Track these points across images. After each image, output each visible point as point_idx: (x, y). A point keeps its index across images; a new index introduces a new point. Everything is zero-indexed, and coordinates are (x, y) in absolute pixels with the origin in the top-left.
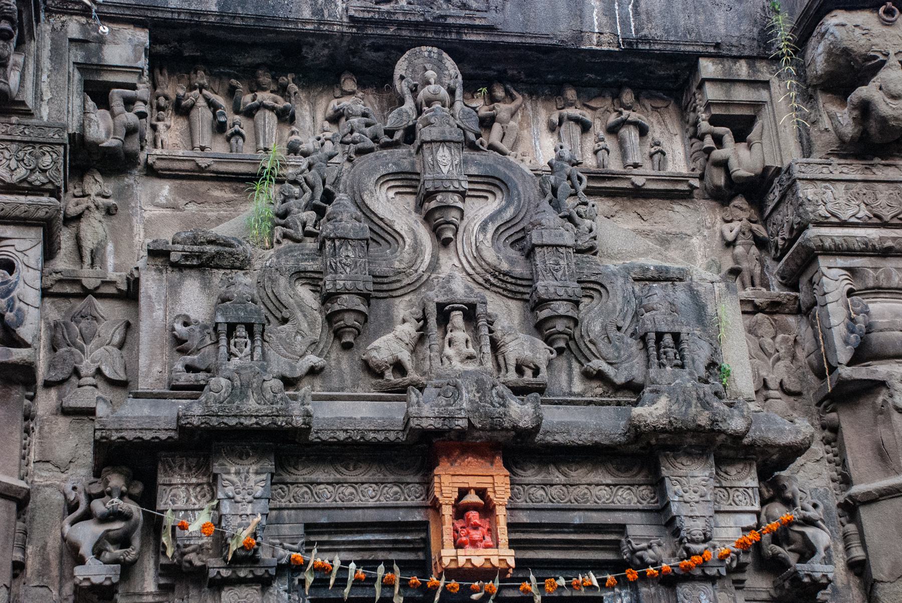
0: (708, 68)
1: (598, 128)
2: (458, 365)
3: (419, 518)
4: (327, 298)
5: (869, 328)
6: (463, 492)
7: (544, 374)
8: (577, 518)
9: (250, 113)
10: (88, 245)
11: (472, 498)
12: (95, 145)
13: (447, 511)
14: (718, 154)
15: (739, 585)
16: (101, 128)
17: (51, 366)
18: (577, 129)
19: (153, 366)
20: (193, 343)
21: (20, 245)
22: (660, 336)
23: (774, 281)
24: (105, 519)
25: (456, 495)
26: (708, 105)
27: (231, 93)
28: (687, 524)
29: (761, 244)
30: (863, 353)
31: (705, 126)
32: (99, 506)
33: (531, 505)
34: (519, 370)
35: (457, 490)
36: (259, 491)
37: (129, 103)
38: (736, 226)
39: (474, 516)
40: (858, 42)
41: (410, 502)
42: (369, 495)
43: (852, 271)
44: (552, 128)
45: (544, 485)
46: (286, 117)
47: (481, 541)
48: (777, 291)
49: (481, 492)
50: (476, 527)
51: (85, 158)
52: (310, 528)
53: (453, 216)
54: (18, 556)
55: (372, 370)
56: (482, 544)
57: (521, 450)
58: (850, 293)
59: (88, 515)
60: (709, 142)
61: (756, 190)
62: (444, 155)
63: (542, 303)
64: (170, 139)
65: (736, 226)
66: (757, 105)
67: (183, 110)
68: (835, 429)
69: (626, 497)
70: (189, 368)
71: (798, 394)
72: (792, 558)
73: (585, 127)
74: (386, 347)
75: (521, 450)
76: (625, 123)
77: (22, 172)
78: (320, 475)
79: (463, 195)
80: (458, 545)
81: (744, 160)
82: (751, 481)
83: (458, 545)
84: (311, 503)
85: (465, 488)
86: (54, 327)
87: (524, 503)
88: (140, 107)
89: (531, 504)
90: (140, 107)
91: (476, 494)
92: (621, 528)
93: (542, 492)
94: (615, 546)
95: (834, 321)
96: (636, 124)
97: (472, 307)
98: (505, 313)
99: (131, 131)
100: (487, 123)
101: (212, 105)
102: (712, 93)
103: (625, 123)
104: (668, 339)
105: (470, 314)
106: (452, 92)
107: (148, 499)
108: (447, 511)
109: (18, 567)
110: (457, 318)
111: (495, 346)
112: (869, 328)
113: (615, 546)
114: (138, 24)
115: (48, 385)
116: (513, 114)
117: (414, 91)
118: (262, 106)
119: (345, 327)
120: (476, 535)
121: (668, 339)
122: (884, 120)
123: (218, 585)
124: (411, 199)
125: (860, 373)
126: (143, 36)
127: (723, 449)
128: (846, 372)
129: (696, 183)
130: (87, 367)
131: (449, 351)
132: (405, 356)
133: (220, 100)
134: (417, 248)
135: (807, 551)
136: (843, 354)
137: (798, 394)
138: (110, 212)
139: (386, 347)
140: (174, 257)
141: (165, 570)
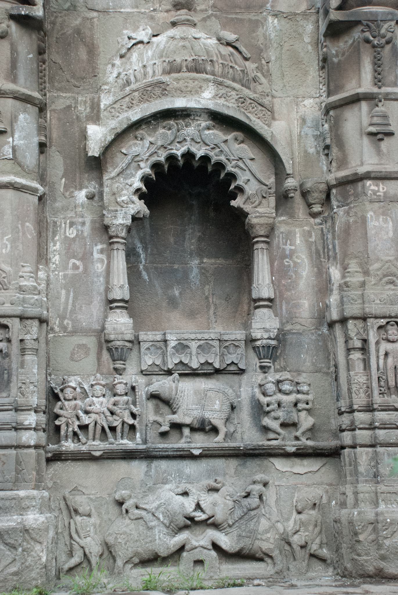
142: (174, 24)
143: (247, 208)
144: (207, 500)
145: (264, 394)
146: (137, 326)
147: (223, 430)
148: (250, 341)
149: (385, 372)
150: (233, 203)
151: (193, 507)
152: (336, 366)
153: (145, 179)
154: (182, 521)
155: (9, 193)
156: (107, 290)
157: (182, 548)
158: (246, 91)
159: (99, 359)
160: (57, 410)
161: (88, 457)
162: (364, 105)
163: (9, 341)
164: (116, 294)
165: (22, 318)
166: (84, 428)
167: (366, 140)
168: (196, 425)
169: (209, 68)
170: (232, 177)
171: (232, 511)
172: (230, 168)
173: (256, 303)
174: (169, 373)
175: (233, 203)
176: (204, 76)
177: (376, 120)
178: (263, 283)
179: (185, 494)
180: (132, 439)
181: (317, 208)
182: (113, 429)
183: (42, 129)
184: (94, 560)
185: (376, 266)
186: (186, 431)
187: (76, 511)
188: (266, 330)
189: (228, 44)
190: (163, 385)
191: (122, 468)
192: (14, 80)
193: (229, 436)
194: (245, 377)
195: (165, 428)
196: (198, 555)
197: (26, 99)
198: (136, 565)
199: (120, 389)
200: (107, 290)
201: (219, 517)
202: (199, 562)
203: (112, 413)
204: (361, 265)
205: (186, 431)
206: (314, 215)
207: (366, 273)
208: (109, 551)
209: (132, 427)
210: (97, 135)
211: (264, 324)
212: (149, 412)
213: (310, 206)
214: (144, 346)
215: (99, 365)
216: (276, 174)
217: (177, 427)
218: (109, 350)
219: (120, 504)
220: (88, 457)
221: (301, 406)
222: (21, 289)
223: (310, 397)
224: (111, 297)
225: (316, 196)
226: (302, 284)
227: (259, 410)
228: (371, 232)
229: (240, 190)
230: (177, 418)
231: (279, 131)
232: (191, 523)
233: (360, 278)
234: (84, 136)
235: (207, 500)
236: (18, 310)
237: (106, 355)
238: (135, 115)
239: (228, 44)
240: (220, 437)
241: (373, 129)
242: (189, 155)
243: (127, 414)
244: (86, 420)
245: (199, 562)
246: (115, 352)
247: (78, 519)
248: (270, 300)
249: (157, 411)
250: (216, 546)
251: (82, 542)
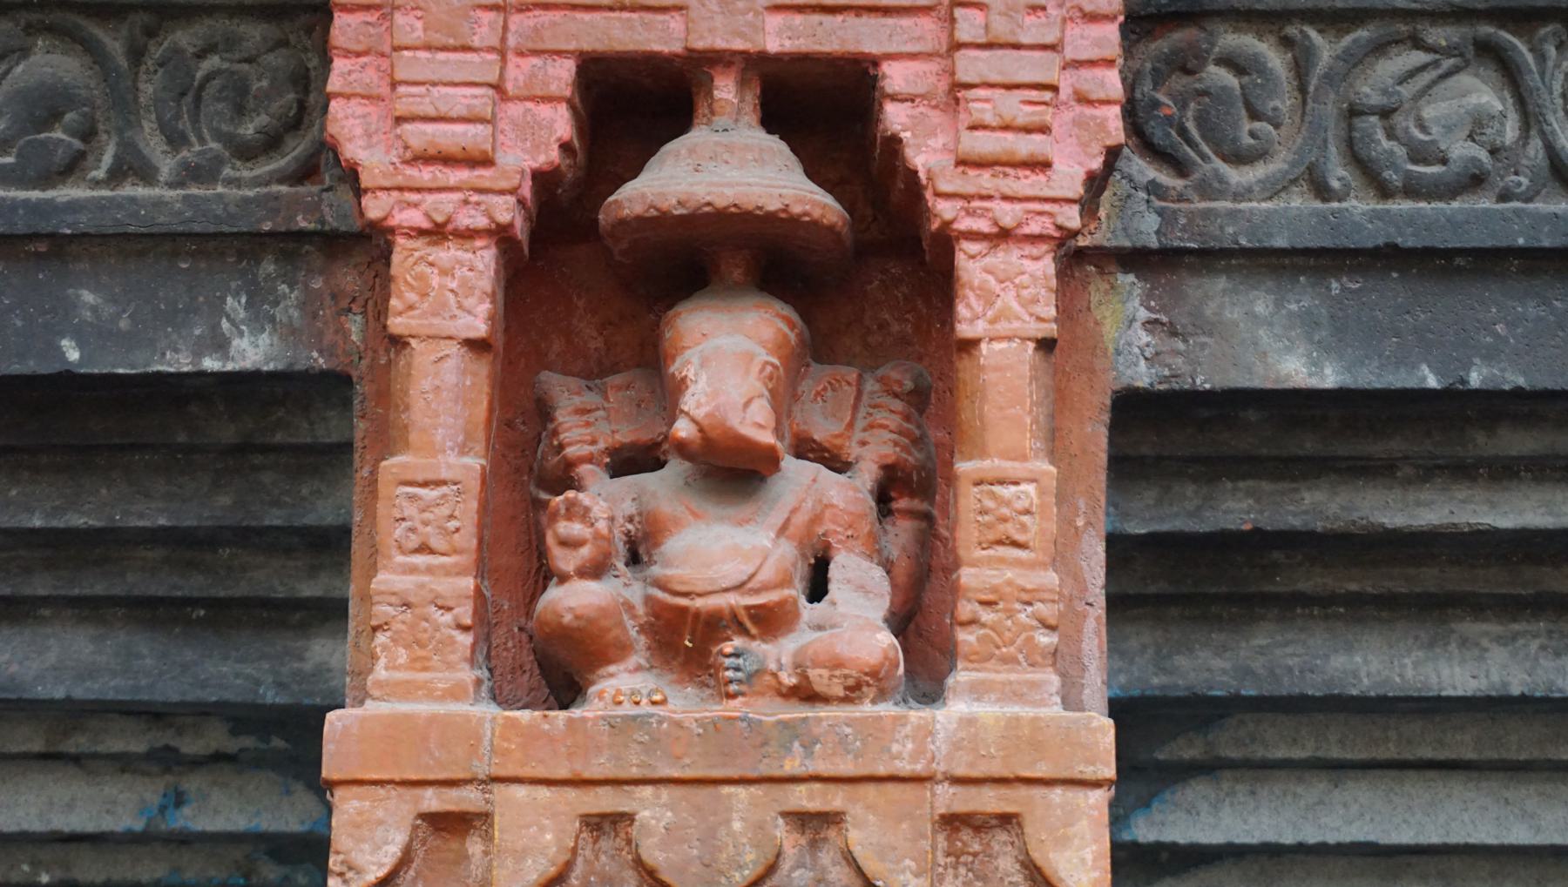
3: (252, 351)
6: (633, 104)
11: (731, 166)
25: (541, 134)
33: (1360, 210)
35: (562, 74)
39: (727, 359)
41: (160, 197)
47: (770, 621)
49: (823, 107)
50: (733, 471)
56: (778, 654)
85: (651, 63)
87: (1299, 202)
89: (1360, 205)
91: (771, 121)
93: (1480, 93)
108: (447, 297)
120: (721, 551)
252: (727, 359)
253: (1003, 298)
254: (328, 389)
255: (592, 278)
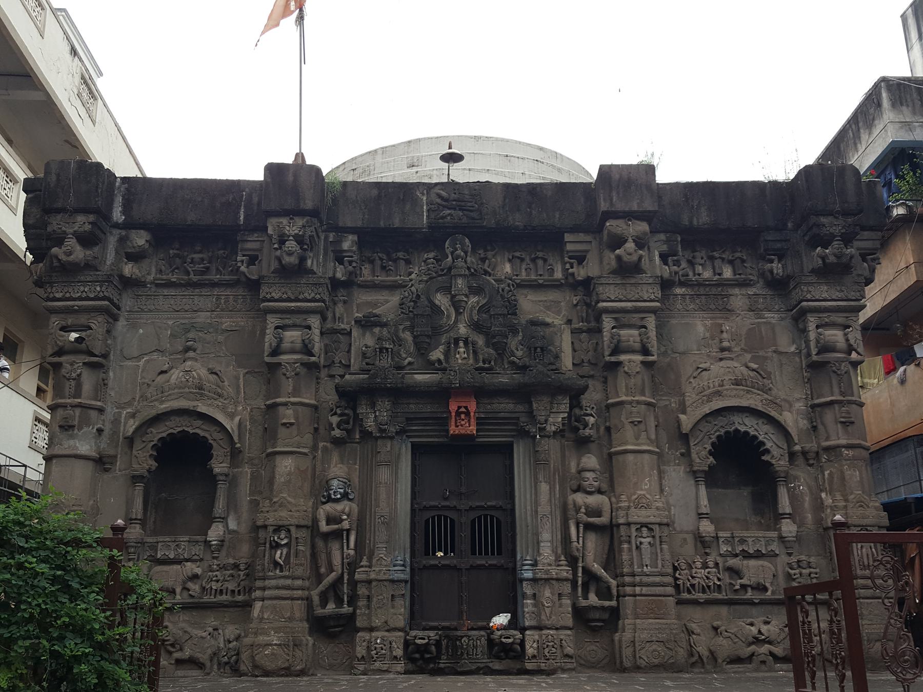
0: (568, 237)
1: (528, 260)
2: (460, 361)
4: (415, 337)
5: (619, 341)
6: (459, 407)
7: (493, 363)
8: (502, 415)
9: (395, 261)
10: (337, 315)
11: (463, 410)
12: (339, 280)
13: (453, 414)
14: (571, 270)
15: (563, 436)
16: (339, 275)
17: (325, 360)
18: (518, 261)
19: (356, 363)
20: (368, 355)
21: (313, 320)
22: (536, 349)
23: (592, 319)
24: (340, 415)
26: (568, 252)
27: (388, 254)
28: (539, 418)
29: (588, 305)
30: (616, 351)
31: (566, 259)
32: (339, 412)
34: (484, 362)
36: (388, 407)
37: (350, 263)
38: (578, 298)
39: (463, 416)
40: (619, 231)
42: (427, 409)
43: (615, 319)
44: (510, 261)
45: (489, 404)
46: (408, 262)
48: (593, 324)
49: (466, 408)
51: (335, 284)
52: (408, 419)
53: (463, 304)
54: (316, 426)
55: (432, 363)
57: (481, 393)
58: (613, 328)
59: (335, 414)
60: (568, 266)
61: (587, 285)
62: (460, 281)
63: (494, 337)
64: (366, 274)
65: (578, 298)
66: (587, 251)
67: (372, 262)
68: (606, 378)
69: (520, 408)
70: (367, 364)
71: (595, 364)
72: (581, 427)
73: (522, 260)
74: (437, 354)
75: (481, 393)
76: (537, 258)
77: (313, 295)
78: (412, 401)
79: (466, 296)
80: (457, 426)
81: (581, 273)
82: (567, 401)
83: (457, 426)
84: (407, 410)
86: (326, 345)
88: (354, 264)
90: (354, 264)
92: (518, 418)
94: (516, 424)
95: (605, 339)
96: (542, 258)
97: (466, 339)
98: (480, 341)
99: (351, 273)
100: (483, 260)
101: (381, 259)
102: (569, 247)
103: (537, 258)
104: (539, 349)
105: (466, 342)
106: (466, 253)
107: (354, 409)
108: (453, 414)
109: (316, 430)
110: (461, 344)
111: (475, 353)
112: (619, 341)
113: (516, 424)
114: (353, 233)
115: (324, 366)
116: (494, 256)
117: (452, 253)
118: (399, 258)
119: (422, 349)
120: (463, 423)
121: (539, 349)
122: (625, 263)
123: (377, 438)
124: (449, 296)
125: (613, 359)
126: (356, 238)
127: (556, 390)
128: (607, 358)
129: (563, 282)
130: (337, 360)
131: (458, 356)
132: (442, 357)
133: (385, 257)
134: (449, 317)
135: (586, 425)
136: (607, 353)
137: (595, 364)
138: (345, 302)
139: (437, 354)
140: (363, 323)
141: (361, 432)
142: (721, 359)
143: (773, 461)
144: (764, 628)
145: (792, 569)
146: (717, 529)
147: (770, 589)
148: (781, 538)
149: (862, 557)
150: (763, 458)
151: (756, 632)
152: (831, 553)
153: (713, 444)
154: (751, 639)
155: (646, 456)
156: (698, 507)
157: (753, 654)
158: (766, 396)
159: (696, 546)
160: (677, 575)
161: (695, 602)
162: (836, 407)
163: (653, 537)
164: (704, 510)
165: (660, 524)
166: (693, 586)
167: (839, 425)
168: (755, 585)
169: (744, 383)
170: (763, 444)
171: (779, 635)
172: (761, 438)
173: (781, 516)
174: (736, 556)
175: (763, 458)
176: (741, 387)
177: (843, 415)
178: (785, 504)
179: (752, 624)
180: (720, 592)
181: (811, 462)
182: (709, 587)
183: (656, 418)
184: (705, 660)
185: (852, 496)
186: (749, 589)
187: (693, 633)
188: (790, 532)
189: (753, 370)
190: (732, 562)
191: (713, 610)
192: (644, 396)
193: (773, 593)
194: (779, 558)
195: (738, 587)
196: (762, 658)
197: (649, 404)
198: (728, 663)
199: (711, 564)
200: (698, 507)
201: (773, 637)
202: (763, 662)
203: (708, 578)
204: (842, 495)
205: (749, 589)
206: (811, 465)
207: (846, 500)
208: (713, 655)
209: (719, 586)
210: (686, 421)
211: (788, 528)
212: (726, 578)
213: (807, 460)
214: (721, 540)
215: (696, 550)
216: (787, 442)
217: (744, 587)
218: (701, 542)
219: (716, 629)
220: (695, 602)
221: (813, 575)
222: (657, 508)
223: (818, 570)
224: (700, 512)
225: (812, 455)
226: (807, 505)
227: (789, 577)
228: (847, 477)
229: (767, 451)
230: (743, 581)
231: (788, 419)
232: (757, 641)
233: (843, 504)
234: (678, 422)
235: (764, 628)
236: (658, 520)
237: (699, 545)
238: (707, 409)
239: (753, 370)
240: (769, 593)
241: (842, 420)
242: (737, 431)
243: (716, 579)
244: (695, 582)
245: (763, 662)
246: (702, 543)
247: (694, 636)
248: (789, 514)
249: (731, 578)
250: (771, 654)
251: (698, 649)
252: (463, 416)
253: (472, 414)
254: (447, 418)
255: (458, 414)
